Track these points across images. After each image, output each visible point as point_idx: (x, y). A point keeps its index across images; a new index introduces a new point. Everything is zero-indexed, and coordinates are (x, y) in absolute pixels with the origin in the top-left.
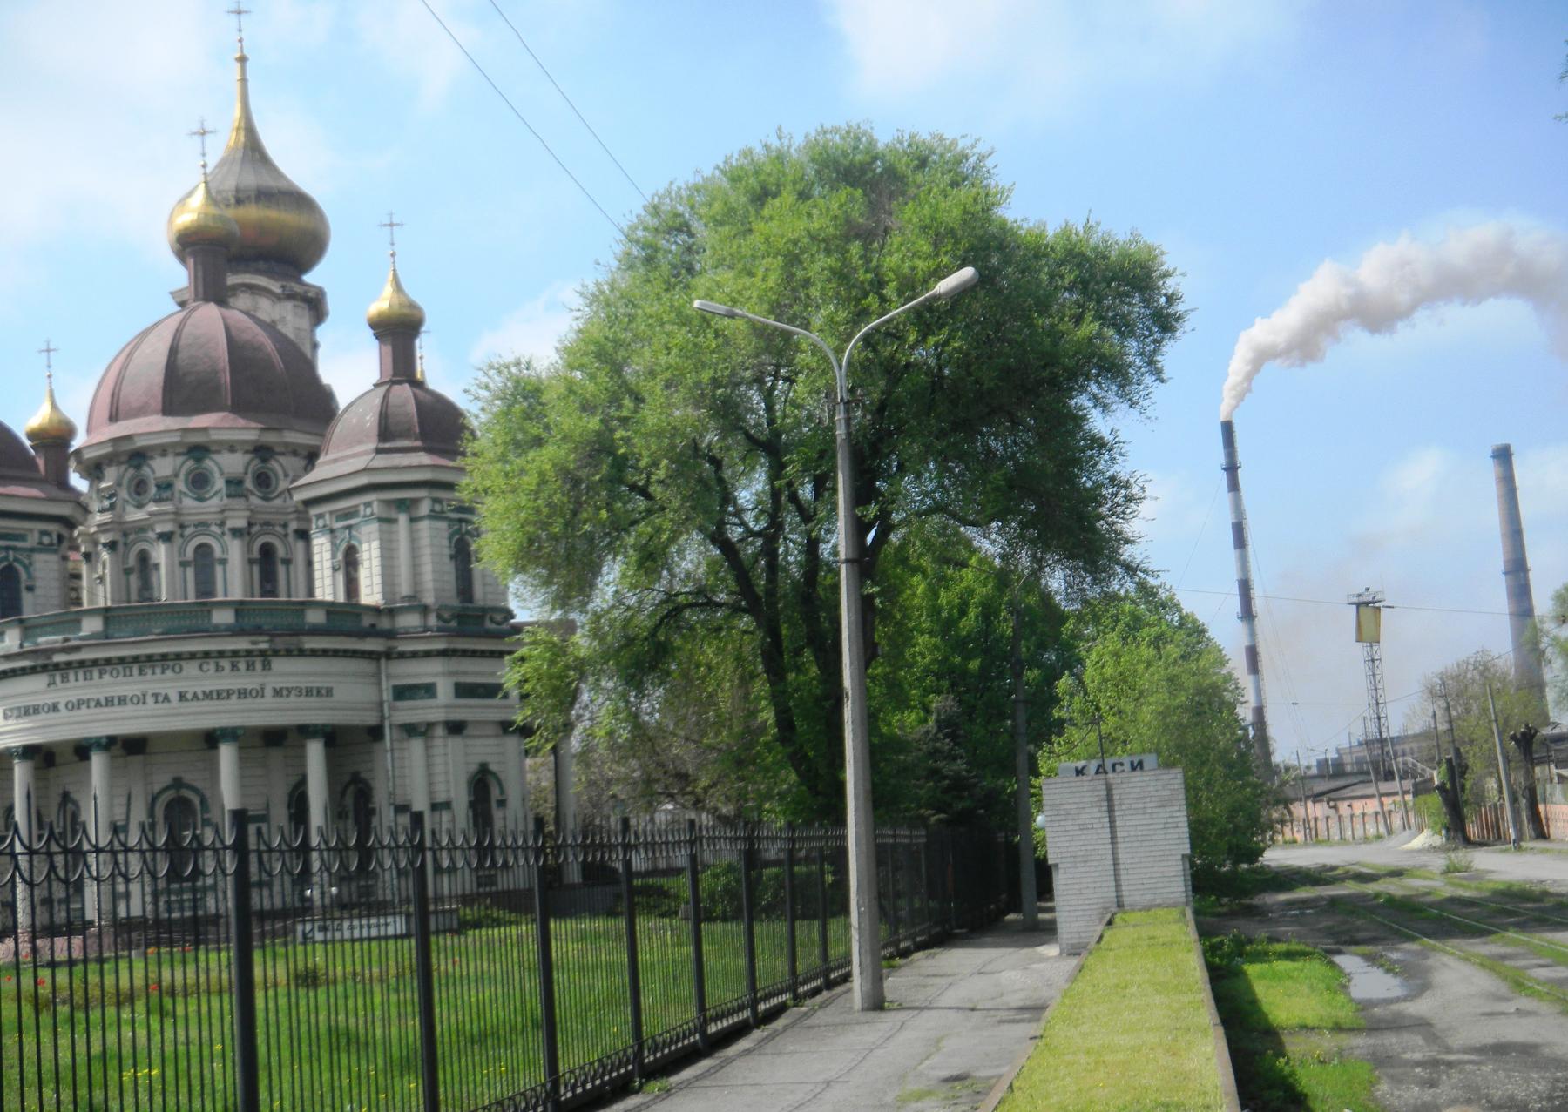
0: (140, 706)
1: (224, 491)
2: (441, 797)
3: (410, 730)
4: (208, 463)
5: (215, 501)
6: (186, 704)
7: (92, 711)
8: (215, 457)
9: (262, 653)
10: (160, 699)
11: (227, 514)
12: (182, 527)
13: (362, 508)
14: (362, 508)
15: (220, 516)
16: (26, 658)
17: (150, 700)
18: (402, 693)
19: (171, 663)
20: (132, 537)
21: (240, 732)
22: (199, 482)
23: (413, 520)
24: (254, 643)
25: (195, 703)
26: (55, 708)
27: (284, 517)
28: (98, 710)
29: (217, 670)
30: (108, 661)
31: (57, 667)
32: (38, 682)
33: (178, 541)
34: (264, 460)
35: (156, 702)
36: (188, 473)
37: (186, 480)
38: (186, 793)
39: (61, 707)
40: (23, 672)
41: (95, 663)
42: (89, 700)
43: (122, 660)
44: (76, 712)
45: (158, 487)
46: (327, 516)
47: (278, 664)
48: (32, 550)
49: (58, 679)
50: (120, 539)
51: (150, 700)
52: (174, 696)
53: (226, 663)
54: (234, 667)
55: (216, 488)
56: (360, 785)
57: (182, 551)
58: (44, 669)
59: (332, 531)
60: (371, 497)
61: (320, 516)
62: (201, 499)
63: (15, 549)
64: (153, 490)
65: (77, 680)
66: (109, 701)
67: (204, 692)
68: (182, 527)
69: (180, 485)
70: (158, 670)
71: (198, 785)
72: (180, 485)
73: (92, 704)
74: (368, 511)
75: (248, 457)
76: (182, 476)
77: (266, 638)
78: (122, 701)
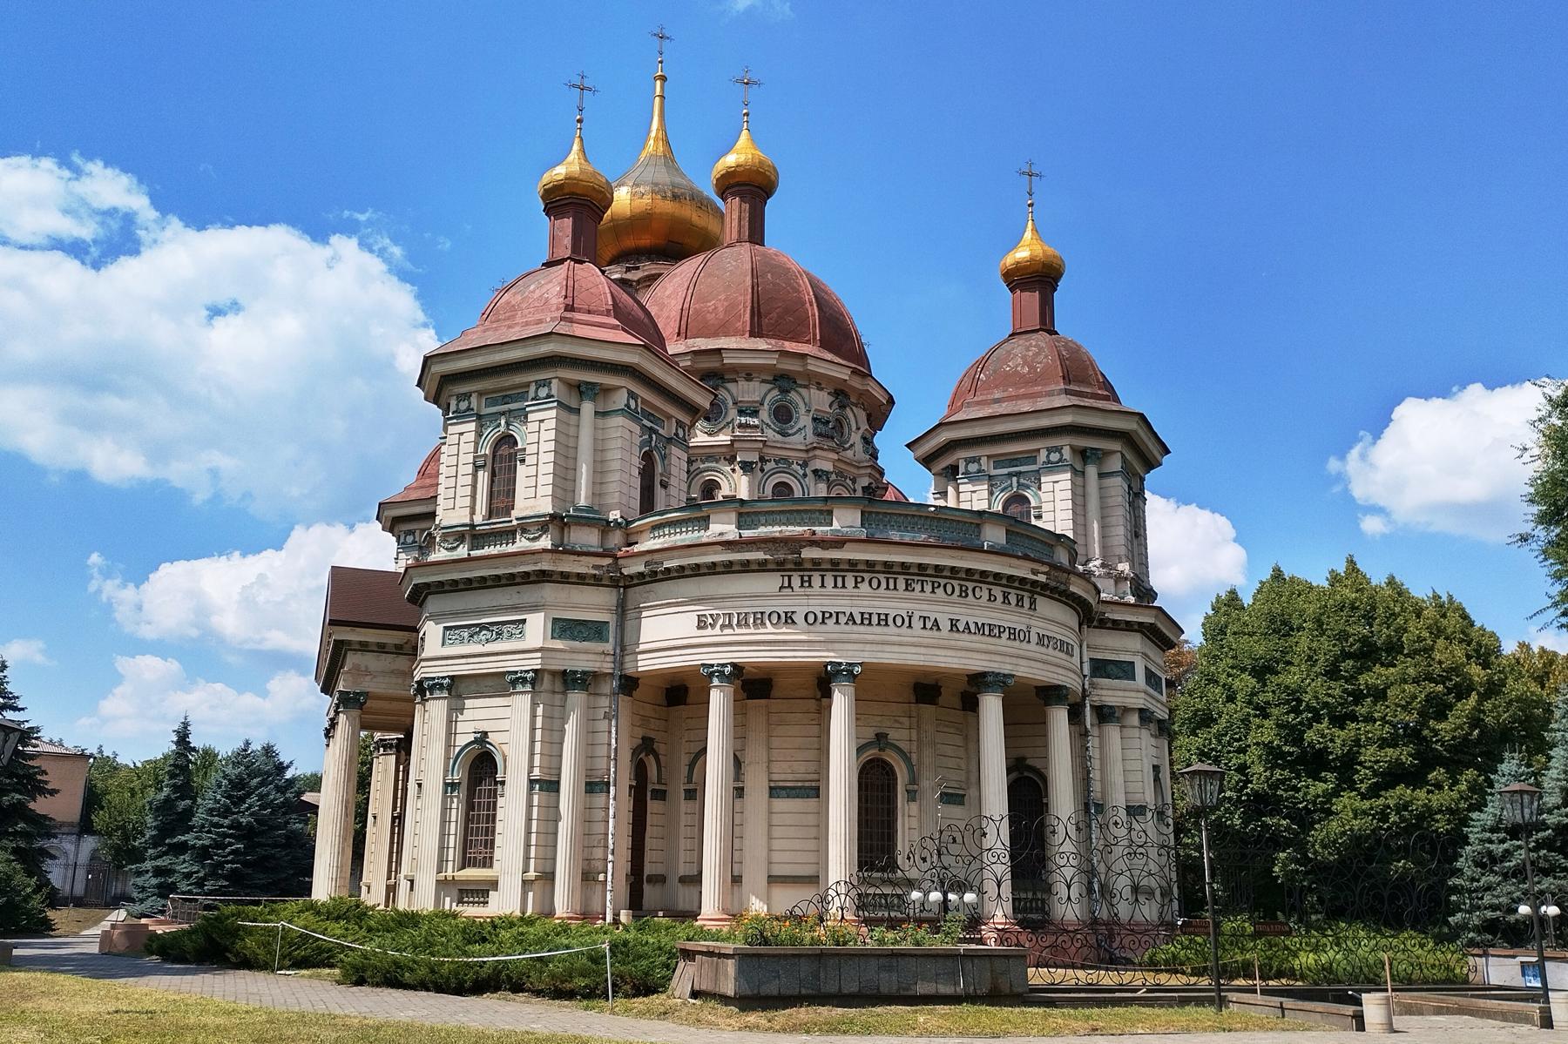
0: (904, 630)
2: (1137, 800)
3: (1105, 714)
4: (793, 395)
5: (798, 438)
6: (956, 635)
7: (843, 627)
8: (803, 391)
9: (1035, 583)
10: (929, 625)
11: (818, 452)
12: (762, 459)
13: (1044, 453)
14: (1044, 453)
15: (803, 455)
16: (758, 549)
17: (918, 624)
18: (1101, 668)
19: (943, 581)
21: (1011, 682)
22: (783, 415)
23: (1101, 475)
24: (1035, 572)
25: (965, 636)
26: (789, 619)
27: (855, 471)
28: (850, 627)
29: (990, 600)
30: (870, 566)
31: (799, 565)
32: (771, 582)
34: (843, 407)
35: (924, 627)
37: (770, 409)
38: (891, 757)
39: (799, 618)
40: (746, 568)
41: (853, 565)
42: (837, 613)
43: (888, 567)
44: (818, 627)
46: (984, 460)
47: (1046, 607)
48: (669, 440)
49: (796, 582)
51: (918, 624)
52: (945, 625)
53: (997, 591)
54: (1005, 597)
55: (800, 425)
56: (1026, 774)
58: (780, 567)
59: (990, 476)
60: (1065, 442)
61: (976, 460)
62: (784, 435)
63: (656, 432)
65: (823, 586)
66: (866, 619)
67: (976, 624)
69: (764, 414)
70: (928, 588)
71: (903, 746)
73: (843, 619)
74: (1055, 457)
75: (832, 399)
76: (766, 406)
77: (1045, 569)
78: (883, 620)
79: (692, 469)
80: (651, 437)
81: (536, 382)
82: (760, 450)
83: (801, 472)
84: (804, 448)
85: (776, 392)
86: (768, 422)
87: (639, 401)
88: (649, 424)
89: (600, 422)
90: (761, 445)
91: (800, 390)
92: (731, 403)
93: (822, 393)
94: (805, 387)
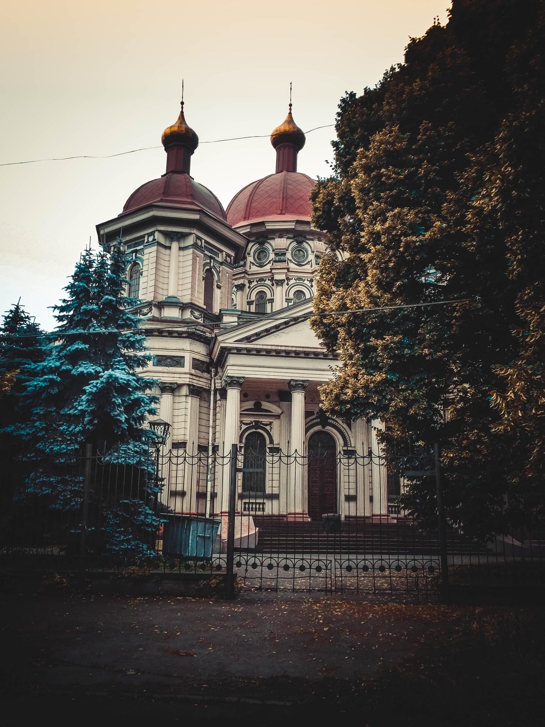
1: (314, 262)
5: (308, 267)
8: (310, 242)
12: (288, 279)
20: (255, 283)
33: (285, 287)
36: (293, 250)
45: (276, 254)
50: (247, 285)
55: (309, 259)
57: (287, 293)
62: (299, 265)
64: (272, 256)
68: (288, 279)
72: (289, 256)
76: (290, 251)
79: (251, 286)
80: (211, 261)
81: (148, 234)
82: (286, 275)
83: (310, 285)
84: (310, 272)
85: (294, 244)
86: (290, 258)
87: (203, 241)
88: (209, 254)
89: (182, 253)
90: (286, 271)
91: (308, 241)
92: (271, 250)
93: (321, 243)
94: (312, 240)
